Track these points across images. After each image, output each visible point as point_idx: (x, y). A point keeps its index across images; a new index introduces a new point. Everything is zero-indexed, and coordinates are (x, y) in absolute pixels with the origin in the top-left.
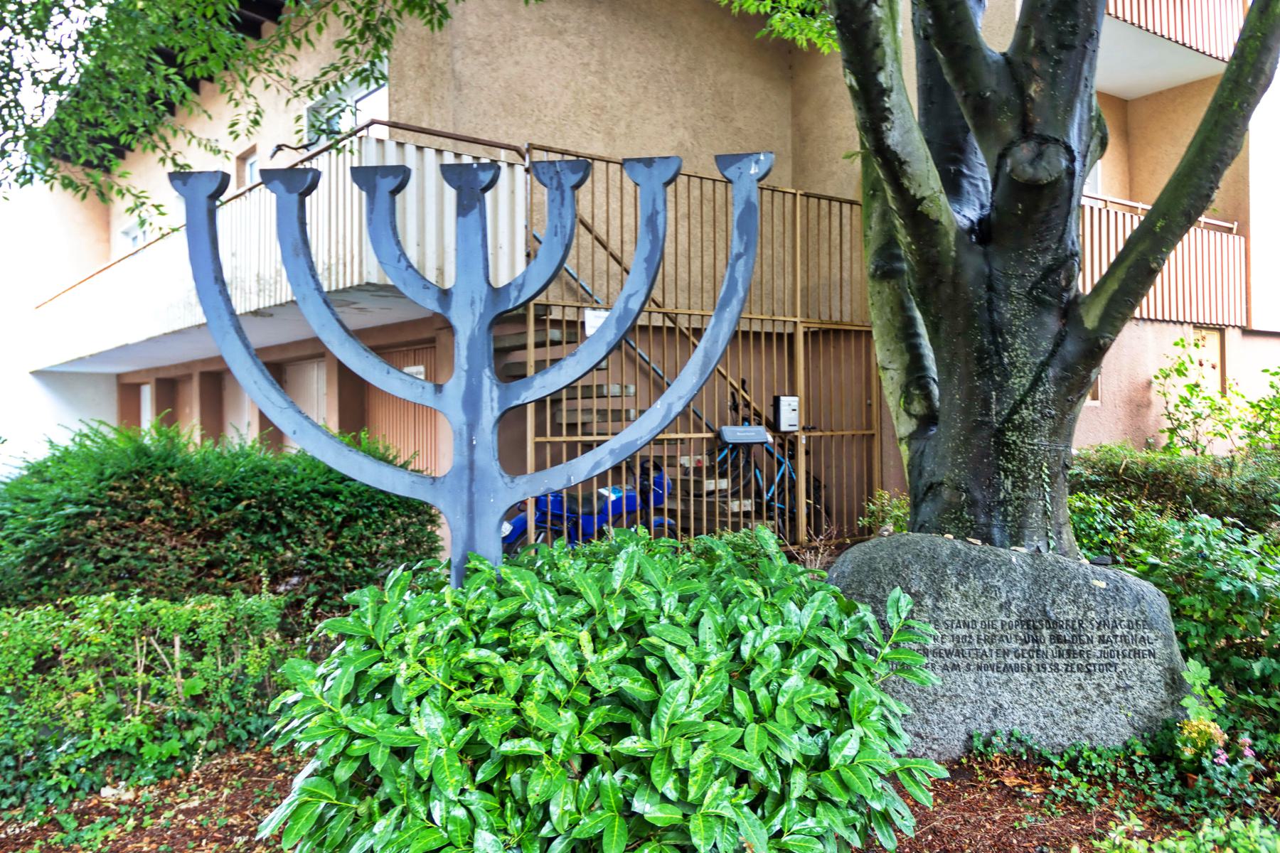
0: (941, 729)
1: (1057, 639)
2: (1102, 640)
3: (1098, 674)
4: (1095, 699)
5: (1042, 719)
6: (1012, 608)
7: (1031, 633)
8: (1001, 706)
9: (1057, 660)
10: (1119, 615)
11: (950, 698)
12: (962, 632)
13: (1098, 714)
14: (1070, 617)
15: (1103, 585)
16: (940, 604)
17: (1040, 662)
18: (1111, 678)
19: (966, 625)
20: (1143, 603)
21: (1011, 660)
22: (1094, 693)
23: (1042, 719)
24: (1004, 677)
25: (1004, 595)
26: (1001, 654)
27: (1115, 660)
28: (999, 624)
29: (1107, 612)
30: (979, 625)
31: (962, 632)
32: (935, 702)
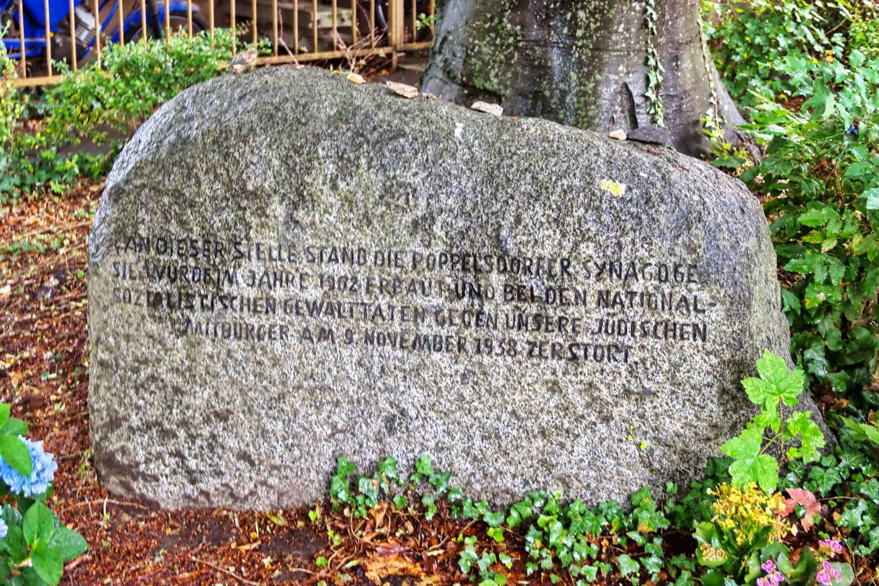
0: (289, 448)
1: (516, 293)
2: (603, 299)
3: (590, 365)
4: (580, 410)
5: (477, 442)
6: (437, 229)
7: (470, 278)
8: (403, 412)
9: (514, 334)
10: (642, 253)
11: (312, 392)
12: (341, 269)
13: (583, 440)
14: (546, 252)
15: (618, 189)
16: (300, 214)
17: (482, 334)
18: (616, 373)
19: (347, 257)
20: (698, 231)
21: (428, 328)
22: (580, 402)
23: (477, 442)
24: (414, 359)
25: (423, 203)
26: (410, 314)
27: (627, 340)
28: (408, 260)
29: (619, 245)
30: (370, 259)
31: (341, 269)
32: (281, 397)
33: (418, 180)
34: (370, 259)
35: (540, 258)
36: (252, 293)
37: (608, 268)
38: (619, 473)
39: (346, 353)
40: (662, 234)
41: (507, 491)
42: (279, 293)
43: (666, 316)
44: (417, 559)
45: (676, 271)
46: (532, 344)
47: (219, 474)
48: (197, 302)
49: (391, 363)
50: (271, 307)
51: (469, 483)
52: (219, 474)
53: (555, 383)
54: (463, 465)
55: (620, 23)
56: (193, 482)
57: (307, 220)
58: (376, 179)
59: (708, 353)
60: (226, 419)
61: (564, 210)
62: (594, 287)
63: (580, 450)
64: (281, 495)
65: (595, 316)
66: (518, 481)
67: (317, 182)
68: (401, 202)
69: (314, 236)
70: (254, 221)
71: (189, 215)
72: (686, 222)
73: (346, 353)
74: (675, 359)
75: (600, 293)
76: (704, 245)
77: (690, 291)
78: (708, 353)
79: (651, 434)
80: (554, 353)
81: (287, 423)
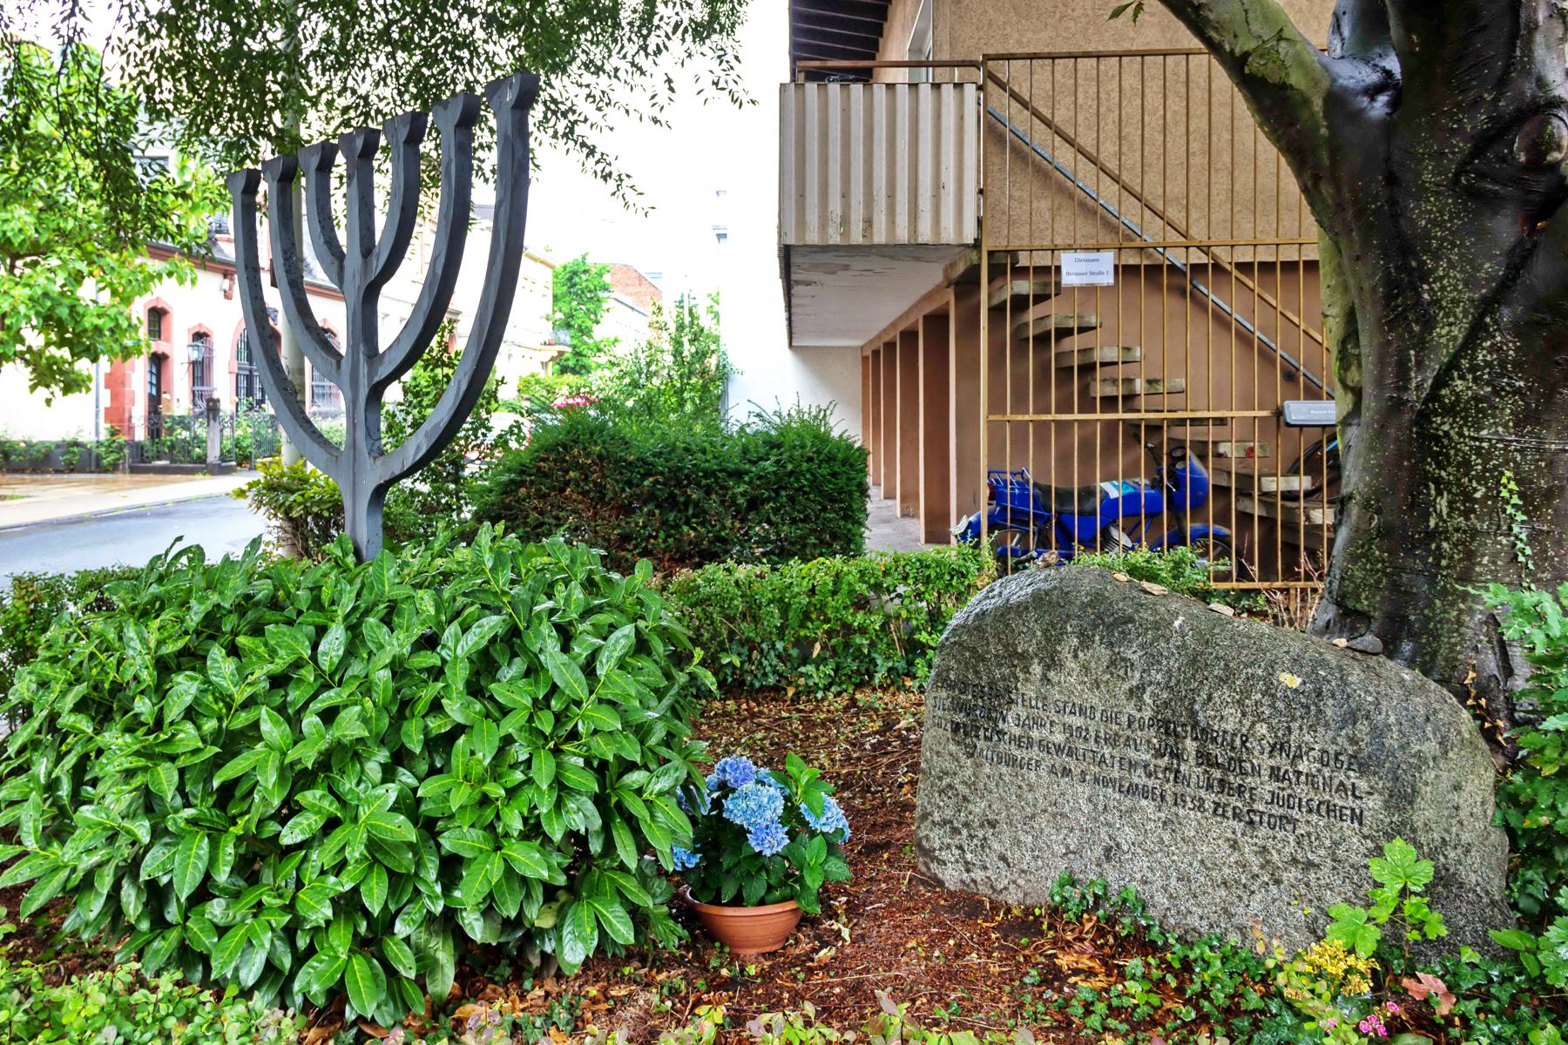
0: (1036, 858)
1: (1204, 758)
2: (1275, 773)
3: (1263, 831)
4: (1256, 869)
5: (1173, 882)
6: (1146, 697)
7: (1171, 741)
8: (1118, 845)
9: (1202, 793)
10: (1307, 738)
11: (1054, 816)
12: (1077, 721)
13: (1258, 897)
14: (1230, 727)
15: (1294, 681)
16: (1051, 674)
17: (1179, 789)
18: (1285, 841)
19: (1082, 712)
20: (1363, 727)
21: (1139, 778)
22: (1255, 862)
23: (1173, 882)
24: (1128, 802)
25: (1137, 675)
26: (1126, 766)
27: (1295, 813)
28: (1124, 719)
29: (1289, 728)
30: (1098, 715)
31: (1077, 721)
32: (1033, 816)
33: (1135, 657)
34: (1098, 715)
35: (1225, 732)
36: (1017, 731)
37: (1279, 747)
38: (1287, 933)
39: (1080, 790)
40: (1327, 725)
41: (1194, 929)
42: (1035, 734)
43: (1327, 797)
44: (1105, 964)
45: (1337, 759)
46: (1217, 805)
47: (985, 868)
48: (981, 733)
49: (1111, 804)
50: (1030, 745)
51: (1165, 916)
52: (985, 868)
53: (1235, 842)
54: (1161, 900)
55: (1483, 555)
56: (968, 871)
57: (1056, 679)
58: (1105, 653)
59: (1365, 837)
60: (994, 827)
61: (1246, 693)
62: (1268, 763)
63: (1255, 905)
64: (1026, 894)
65: (1268, 788)
66: (1204, 923)
67: (1065, 651)
68: (1121, 673)
69: (1060, 692)
70: (1021, 676)
71: (981, 667)
72: (1351, 718)
73: (1080, 790)
74: (1336, 837)
75: (1272, 768)
76: (1367, 739)
77: (1349, 778)
78: (1365, 837)
79: (1316, 903)
80: (1235, 816)
81: (1035, 838)
